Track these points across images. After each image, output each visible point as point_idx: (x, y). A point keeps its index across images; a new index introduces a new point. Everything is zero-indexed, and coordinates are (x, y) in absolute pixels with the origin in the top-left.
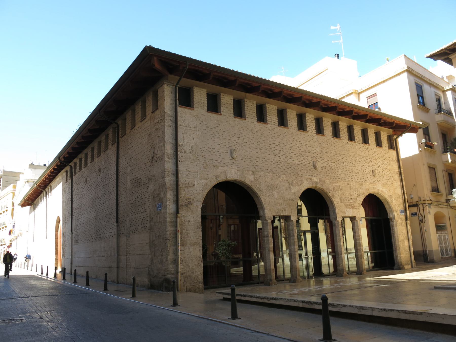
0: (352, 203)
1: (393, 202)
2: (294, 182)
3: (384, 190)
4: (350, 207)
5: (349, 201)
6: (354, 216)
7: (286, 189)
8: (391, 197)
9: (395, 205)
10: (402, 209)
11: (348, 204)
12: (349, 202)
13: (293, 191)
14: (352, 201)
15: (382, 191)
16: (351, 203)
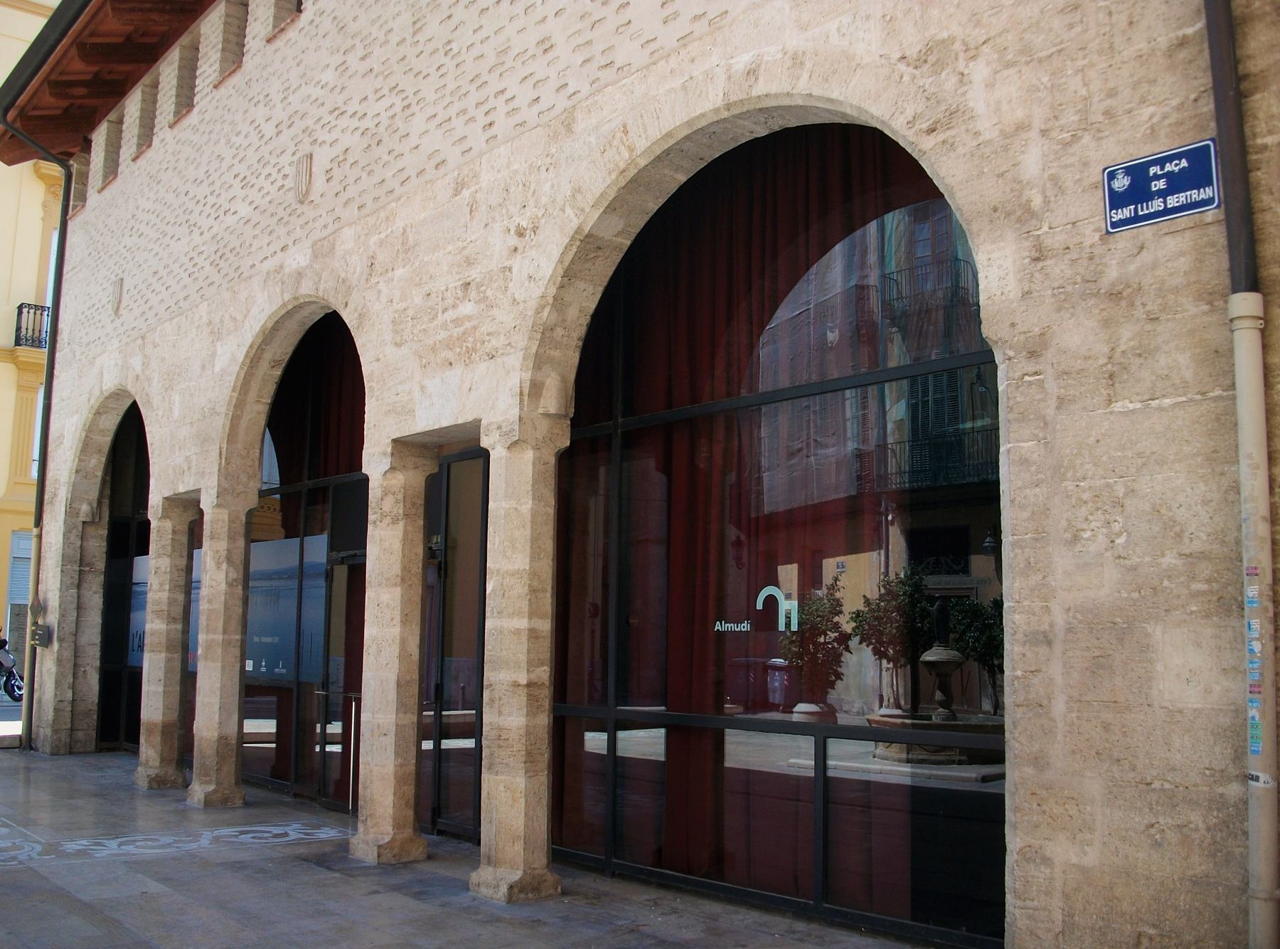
0: (469, 318)
1: (977, 100)
2: (227, 317)
3: (833, 26)
4: (450, 355)
5: (451, 315)
6: (470, 419)
7: (203, 367)
8: (939, 67)
9: (1021, 127)
10: (1142, 151)
11: (443, 335)
12: (444, 326)
13: (217, 369)
14: (467, 308)
15: (797, 61)
16: (457, 322)
